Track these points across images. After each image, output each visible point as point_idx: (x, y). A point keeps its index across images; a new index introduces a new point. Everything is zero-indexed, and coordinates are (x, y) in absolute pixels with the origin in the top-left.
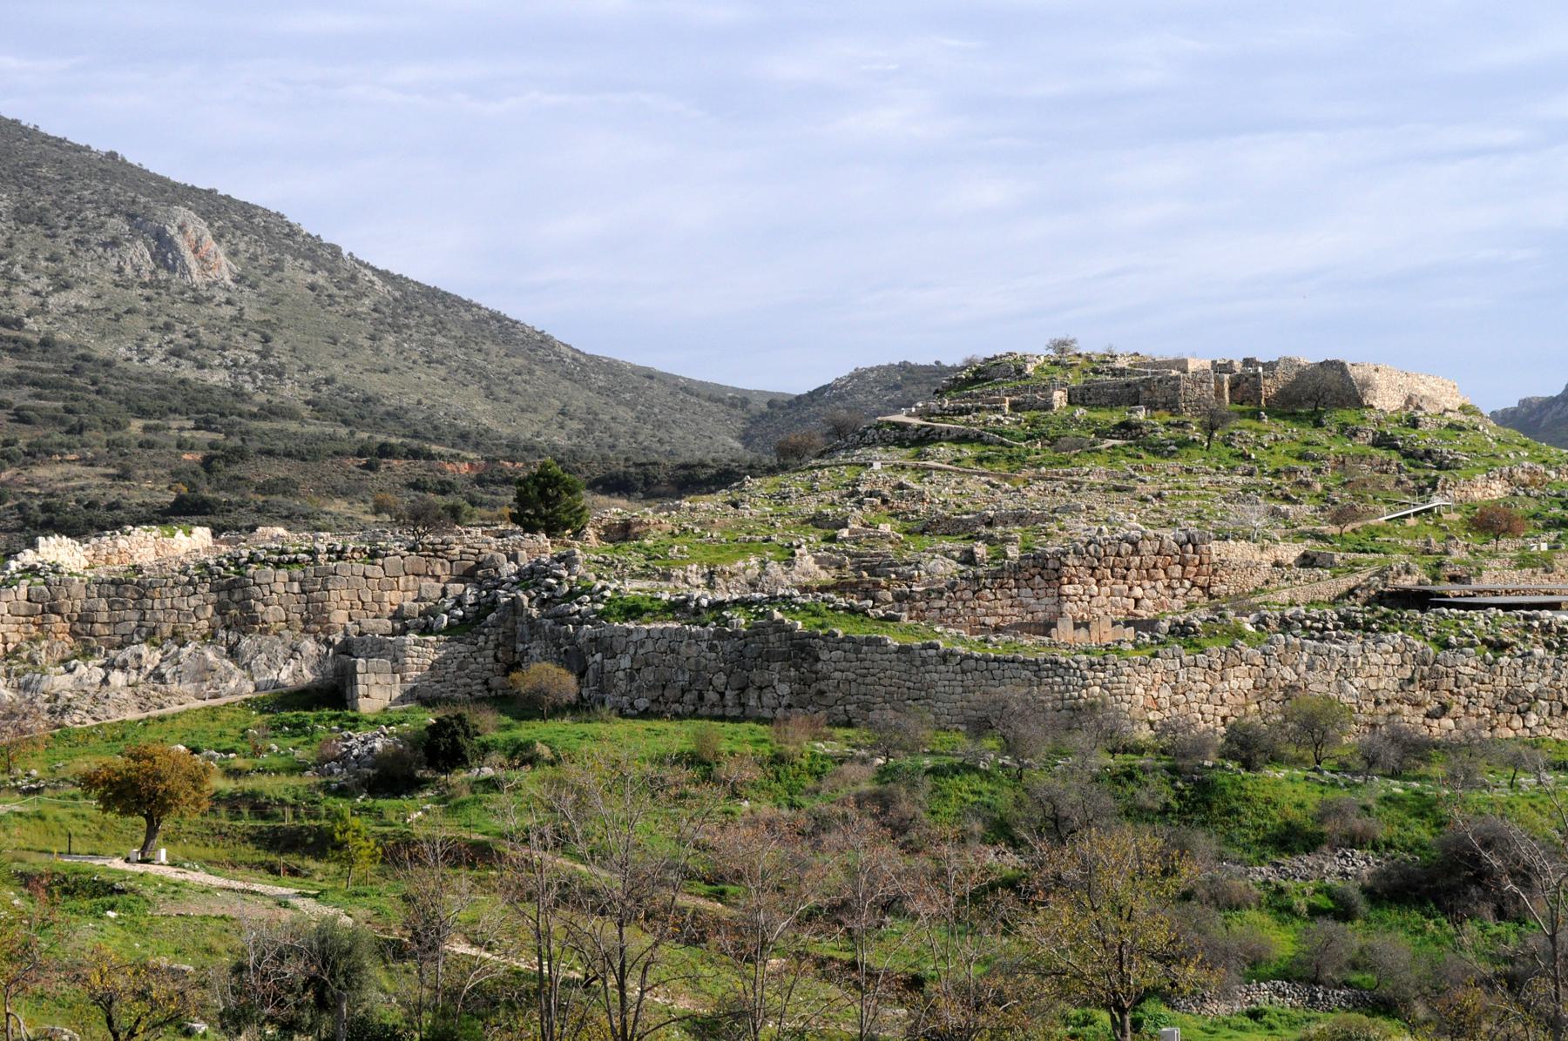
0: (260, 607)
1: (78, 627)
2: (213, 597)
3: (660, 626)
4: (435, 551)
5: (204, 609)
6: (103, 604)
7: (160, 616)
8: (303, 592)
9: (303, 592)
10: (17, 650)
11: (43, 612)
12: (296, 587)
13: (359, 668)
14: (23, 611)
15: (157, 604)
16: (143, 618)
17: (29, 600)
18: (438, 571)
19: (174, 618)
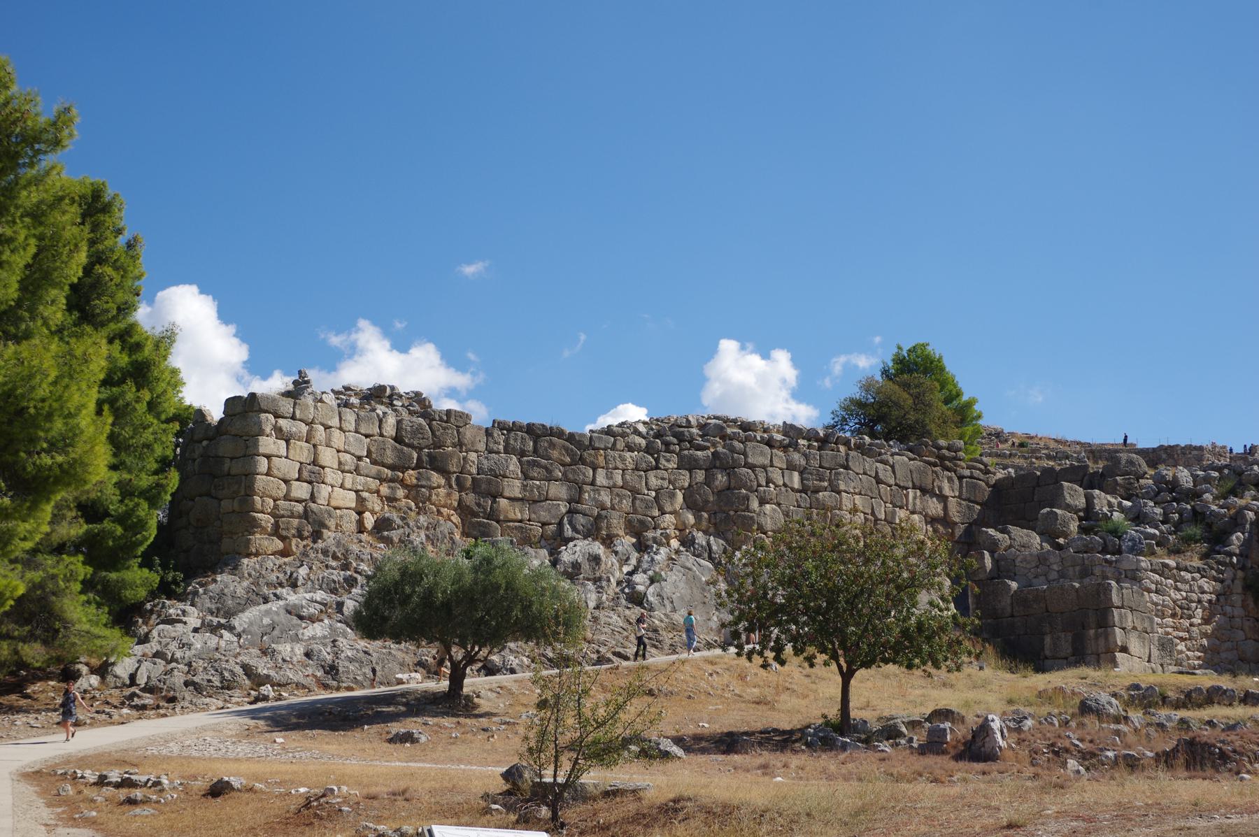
0: (755, 504)
1: (470, 499)
2: (684, 479)
3: (376, 690)
4: (942, 458)
5: (672, 496)
6: (513, 464)
7: (605, 498)
8: (804, 490)
9: (804, 490)
10: (383, 524)
11: (419, 466)
12: (796, 480)
13: (1115, 599)
14: (390, 457)
15: (601, 479)
16: (575, 500)
17: (398, 439)
18: (947, 491)
19: (626, 504)
